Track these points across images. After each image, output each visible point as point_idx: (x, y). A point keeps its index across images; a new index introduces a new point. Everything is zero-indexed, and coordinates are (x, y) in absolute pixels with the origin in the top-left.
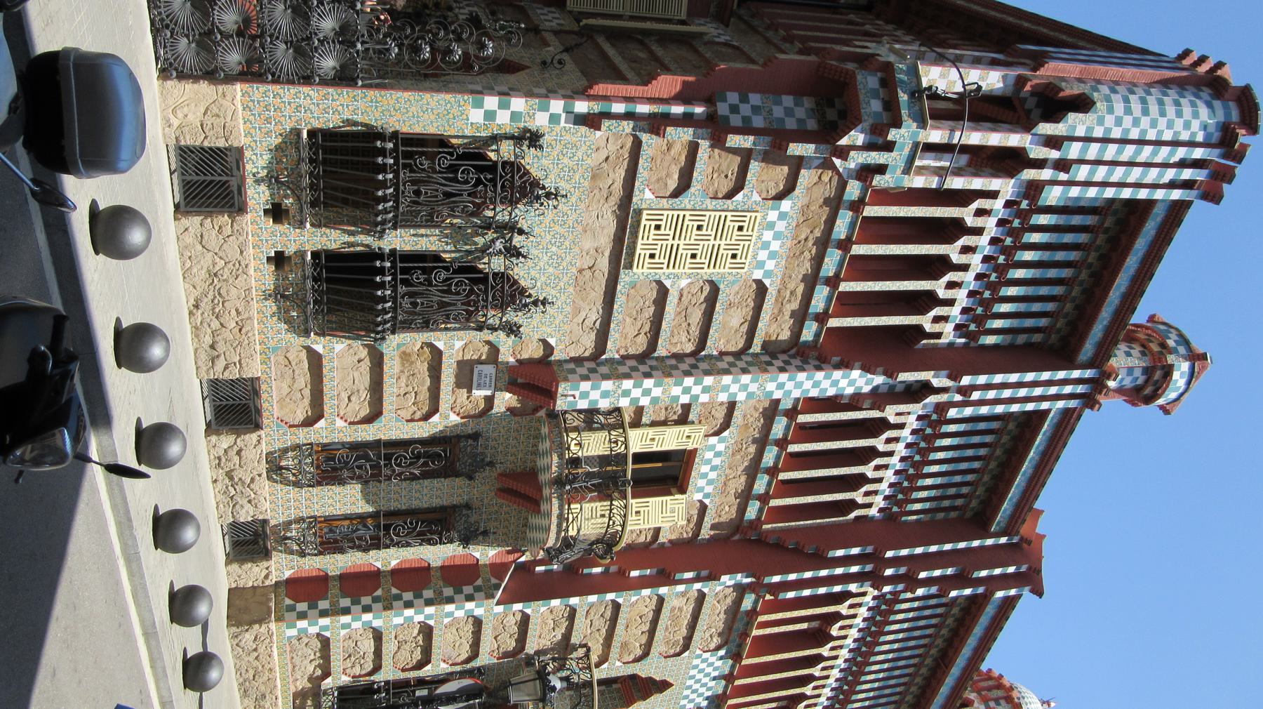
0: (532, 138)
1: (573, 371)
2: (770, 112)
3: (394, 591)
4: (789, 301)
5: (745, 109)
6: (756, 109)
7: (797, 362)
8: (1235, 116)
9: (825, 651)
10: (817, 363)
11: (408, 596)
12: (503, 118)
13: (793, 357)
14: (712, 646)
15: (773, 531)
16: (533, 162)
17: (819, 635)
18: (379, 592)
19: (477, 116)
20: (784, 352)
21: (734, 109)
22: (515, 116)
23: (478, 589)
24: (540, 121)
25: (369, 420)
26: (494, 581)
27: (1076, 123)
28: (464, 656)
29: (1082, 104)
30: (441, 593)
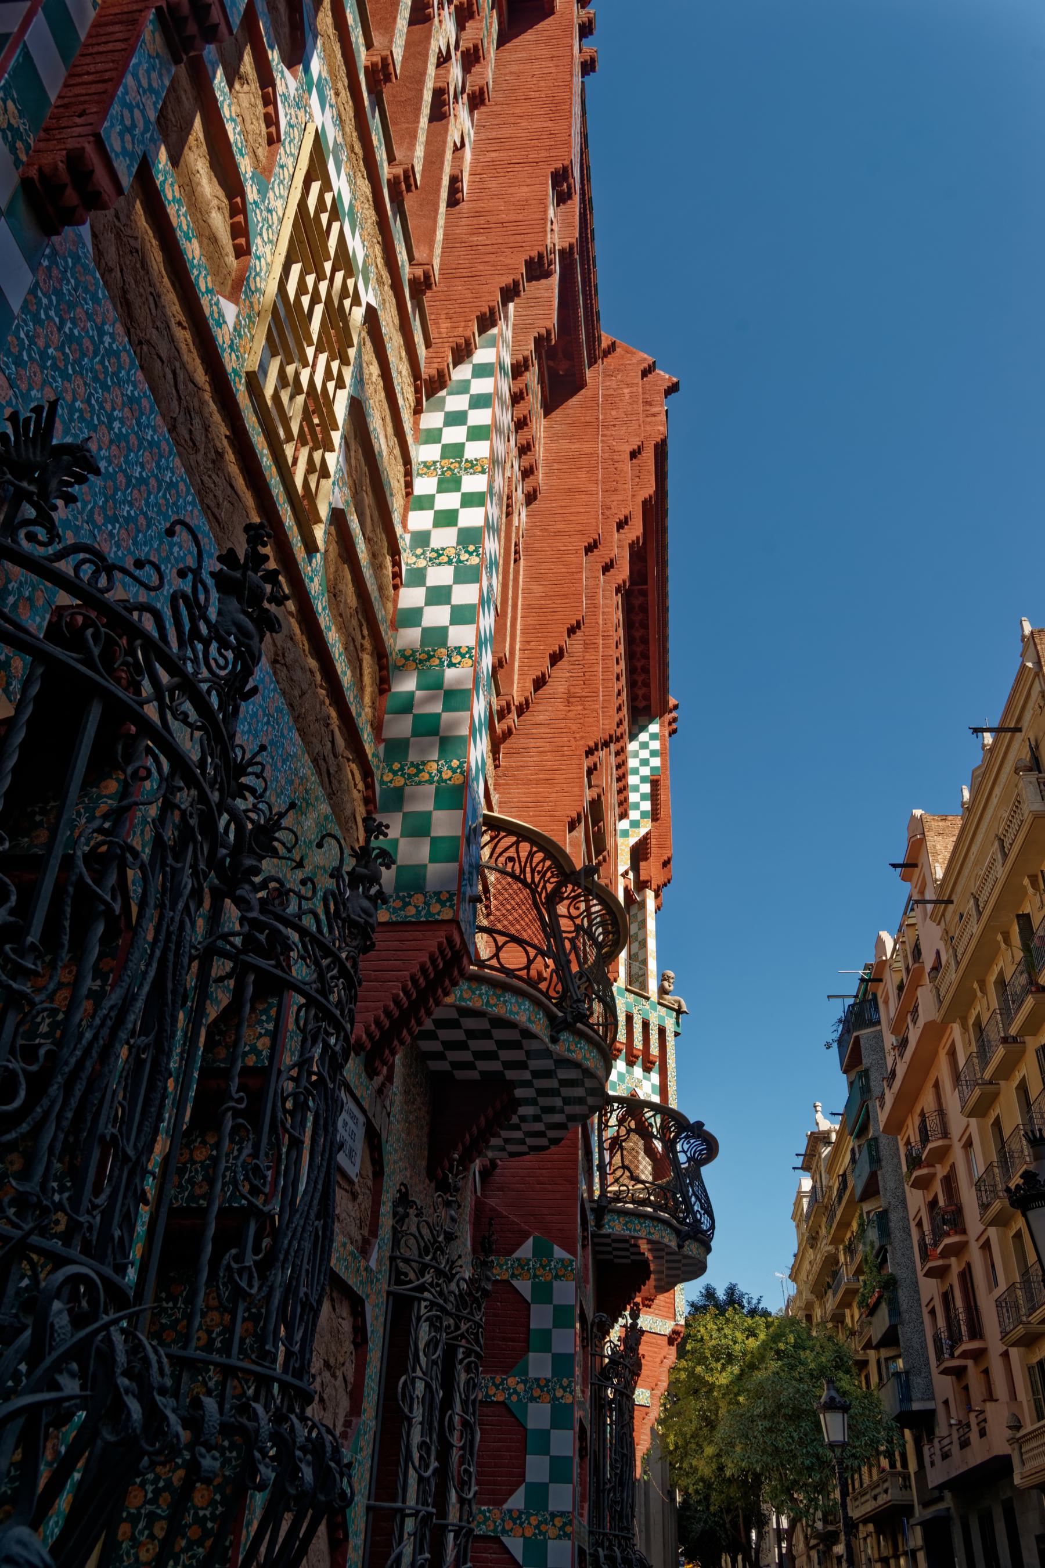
3: (517, 1501)
11: (537, 1468)
15: (523, 689)
26: (526, 1250)
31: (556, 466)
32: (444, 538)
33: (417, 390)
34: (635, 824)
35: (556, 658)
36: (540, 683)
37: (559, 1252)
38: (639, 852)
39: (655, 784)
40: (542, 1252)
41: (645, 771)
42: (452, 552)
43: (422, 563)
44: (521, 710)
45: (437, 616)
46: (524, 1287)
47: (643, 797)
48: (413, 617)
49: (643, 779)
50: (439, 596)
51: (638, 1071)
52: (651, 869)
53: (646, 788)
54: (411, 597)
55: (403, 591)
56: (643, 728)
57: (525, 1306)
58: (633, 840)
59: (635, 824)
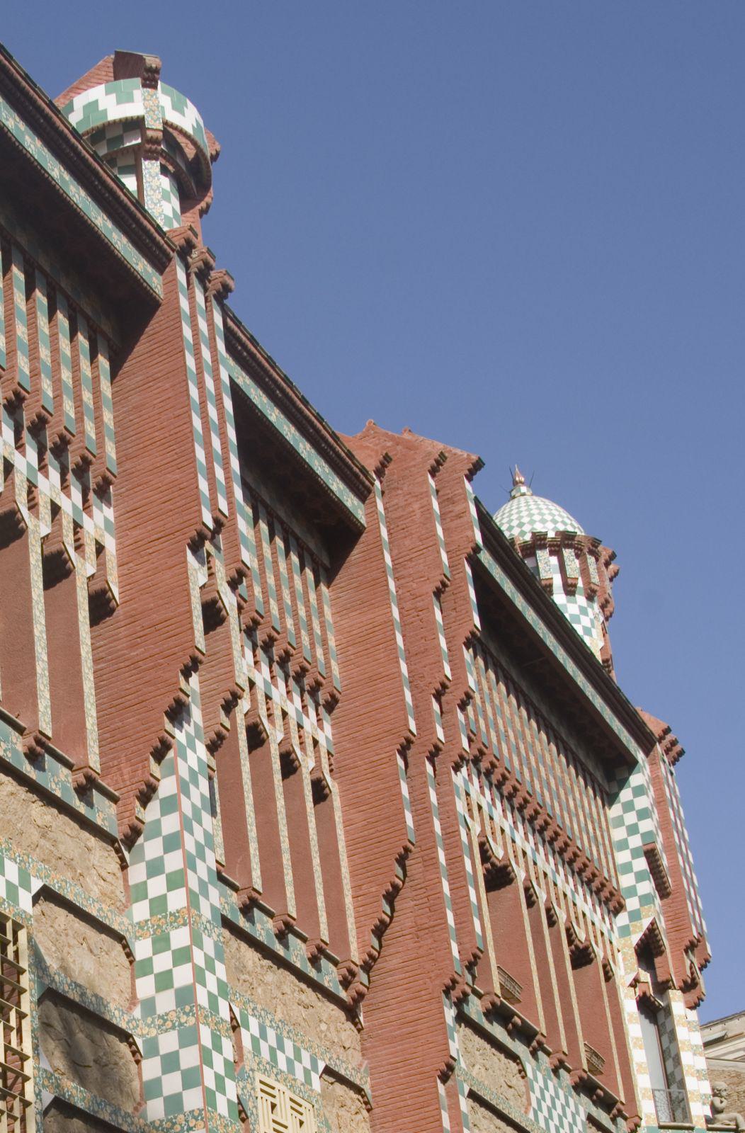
4: (55, 843)
7: (151, 848)
9: (520, 874)
10: (154, 806)
14: (517, 1081)
15: (362, 944)
17: (498, 878)
20: (124, 866)
31: (352, 650)
32: (166, 1002)
33: (118, 851)
34: (635, 916)
35: (391, 898)
36: (380, 930)
38: (648, 950)
39: (651, 855)
41: (635, 841)
42: (173, 1016)
43: (154, 1032)
44: (367, 967)
45: (172, 1084)
47: (640, 877)
48: (153, 1089)
49: (635, 853)
50: (171, 1063)
52: (672, 964)
53: (641, 864)
54: (151, 1068)
55: (145, 1063)
56: (622, 783)
58: (636, 938)
59: (635, 916)
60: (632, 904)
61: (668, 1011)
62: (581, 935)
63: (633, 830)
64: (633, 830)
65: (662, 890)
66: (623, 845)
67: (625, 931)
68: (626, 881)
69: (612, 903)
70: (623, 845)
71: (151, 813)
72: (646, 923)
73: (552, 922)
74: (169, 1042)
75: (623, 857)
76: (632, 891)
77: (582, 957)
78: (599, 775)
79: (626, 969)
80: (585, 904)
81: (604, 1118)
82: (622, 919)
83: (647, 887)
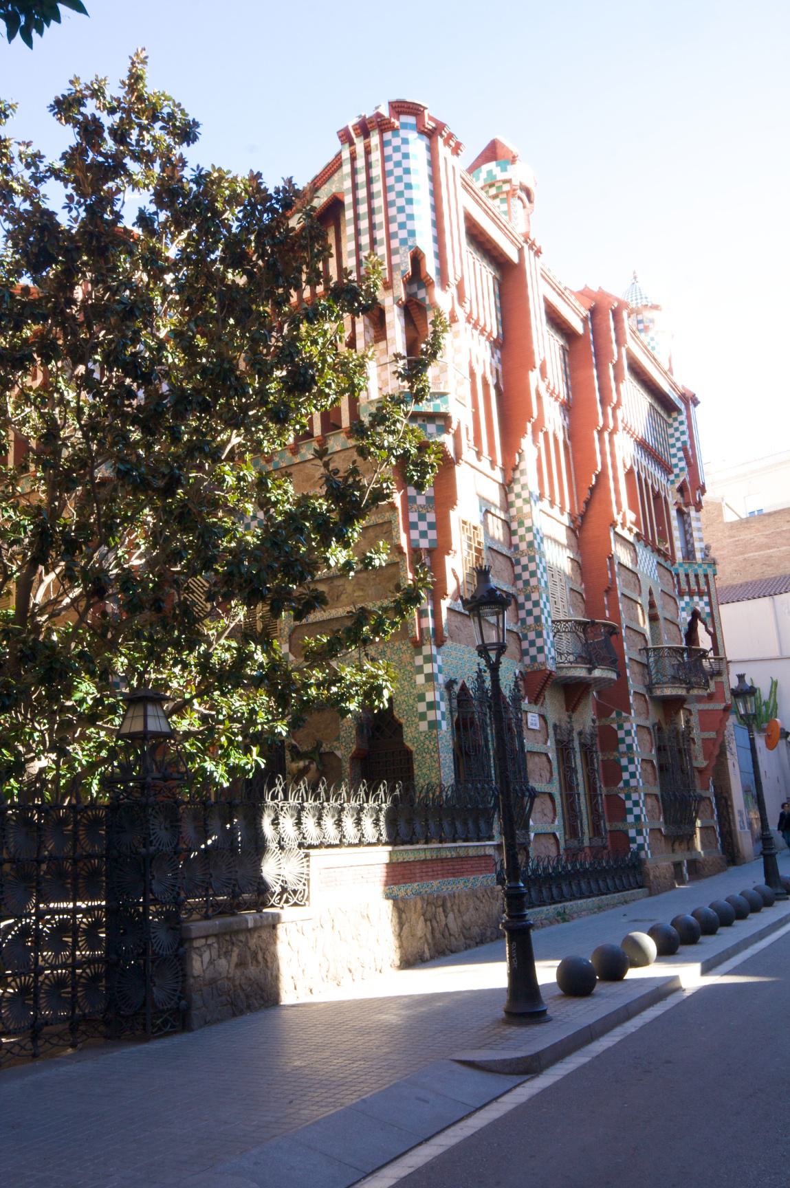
0: (450, 685)
1: (534, 658)
2: (422, 507)
3: (621, 784)
5: (423, 526)
6: (422, 517)
8: (411, 120)
11: (626, 776)
12: (443, 706)
13: (511, 490)
16: (457, 688)
18: (622, 796)
19: (444, 725)
21: (423, 535)
22: (442, 699)
23: (621, 727)
24: (441, 679)
25: (553, 801)
26: (614, 715)
27: (430, 266)
28: (648, 737)
29: (417, 259)
30: (623, 753)
34: (677, 476)
37: (624, 714)
38: (682, 490)
39: (684, 449)
40: (619, 714)
41: (679, 445)
46: (615, 726)
49: (679, 450)
51: (696, 598)
53: (681, 454)
57: (616, 732)
58: (677, 485)
59: (677, 476)
60: (676, 471)
61: (689, 514)
62: (656, 488)
63: (678, 439)
64: (678, 439)
65: (688, 463)
66: (673, 446)
67: (673, 482)
68: (674, 461)
69: (667, 469)
70: (673, 446)
71: (517, 474)
72: (681, 479)
73: (647, 485)
74: (524, 561)
75: (673, 451)
76: (676, 466)
77: (657, 496)
78: (665, 416)
79: (672, 498)
80: (658, 474)
81: (662, 561)
82: (672, 477)
83: (683, 464)
